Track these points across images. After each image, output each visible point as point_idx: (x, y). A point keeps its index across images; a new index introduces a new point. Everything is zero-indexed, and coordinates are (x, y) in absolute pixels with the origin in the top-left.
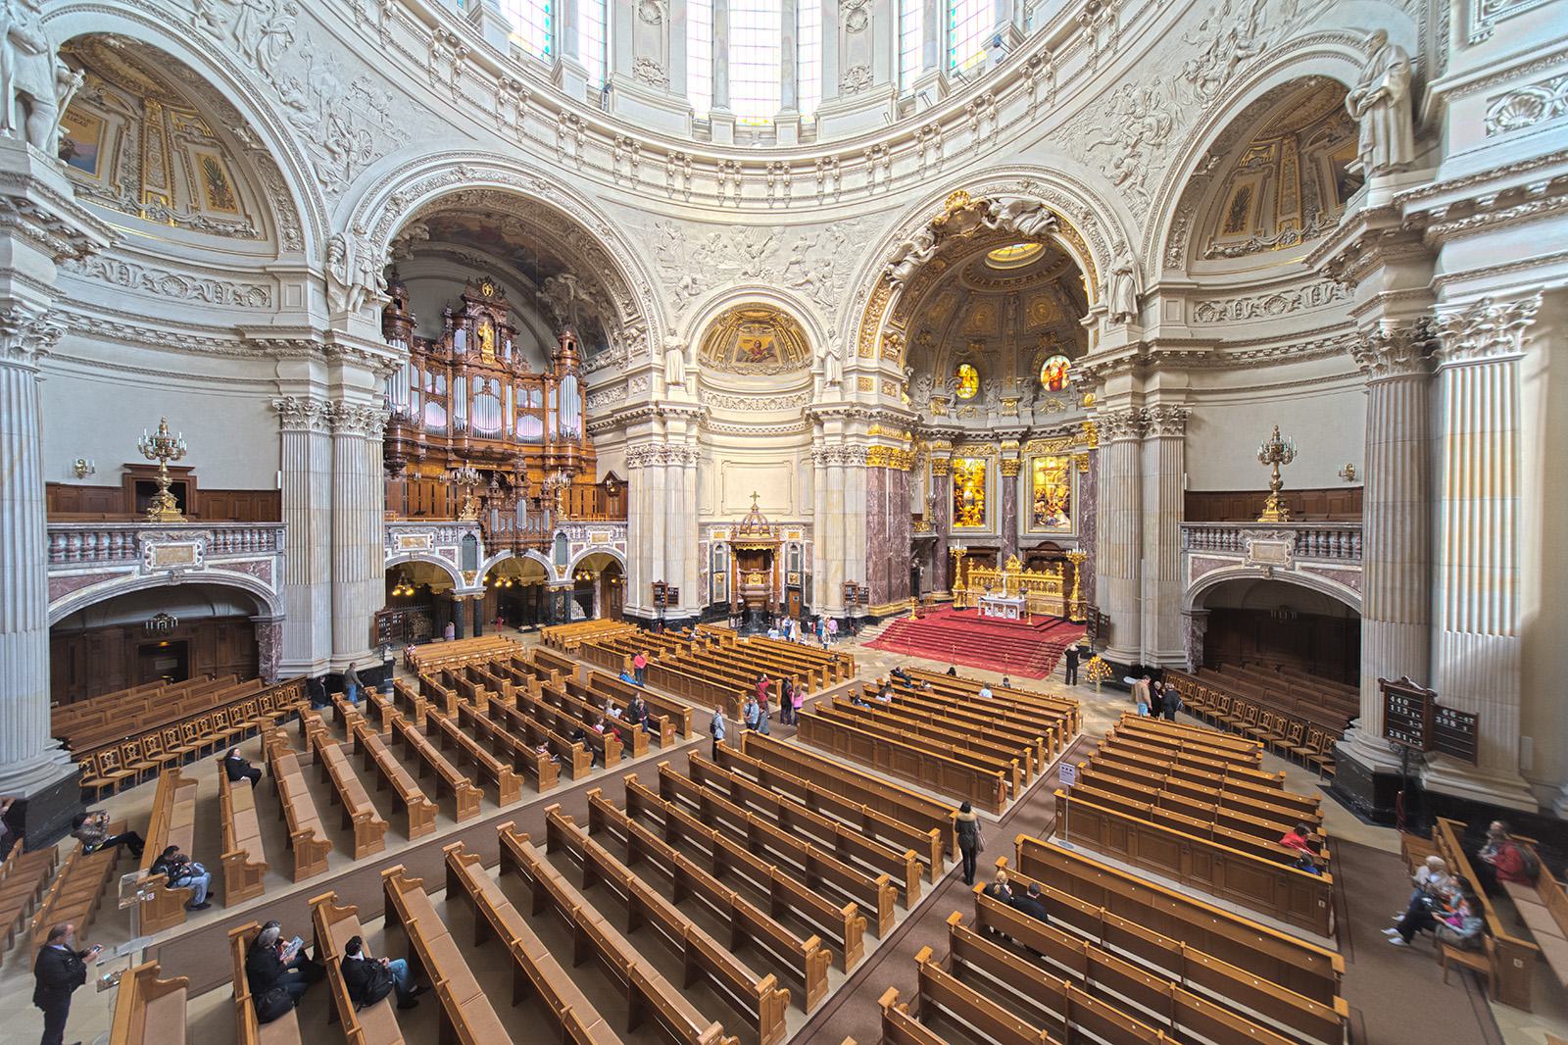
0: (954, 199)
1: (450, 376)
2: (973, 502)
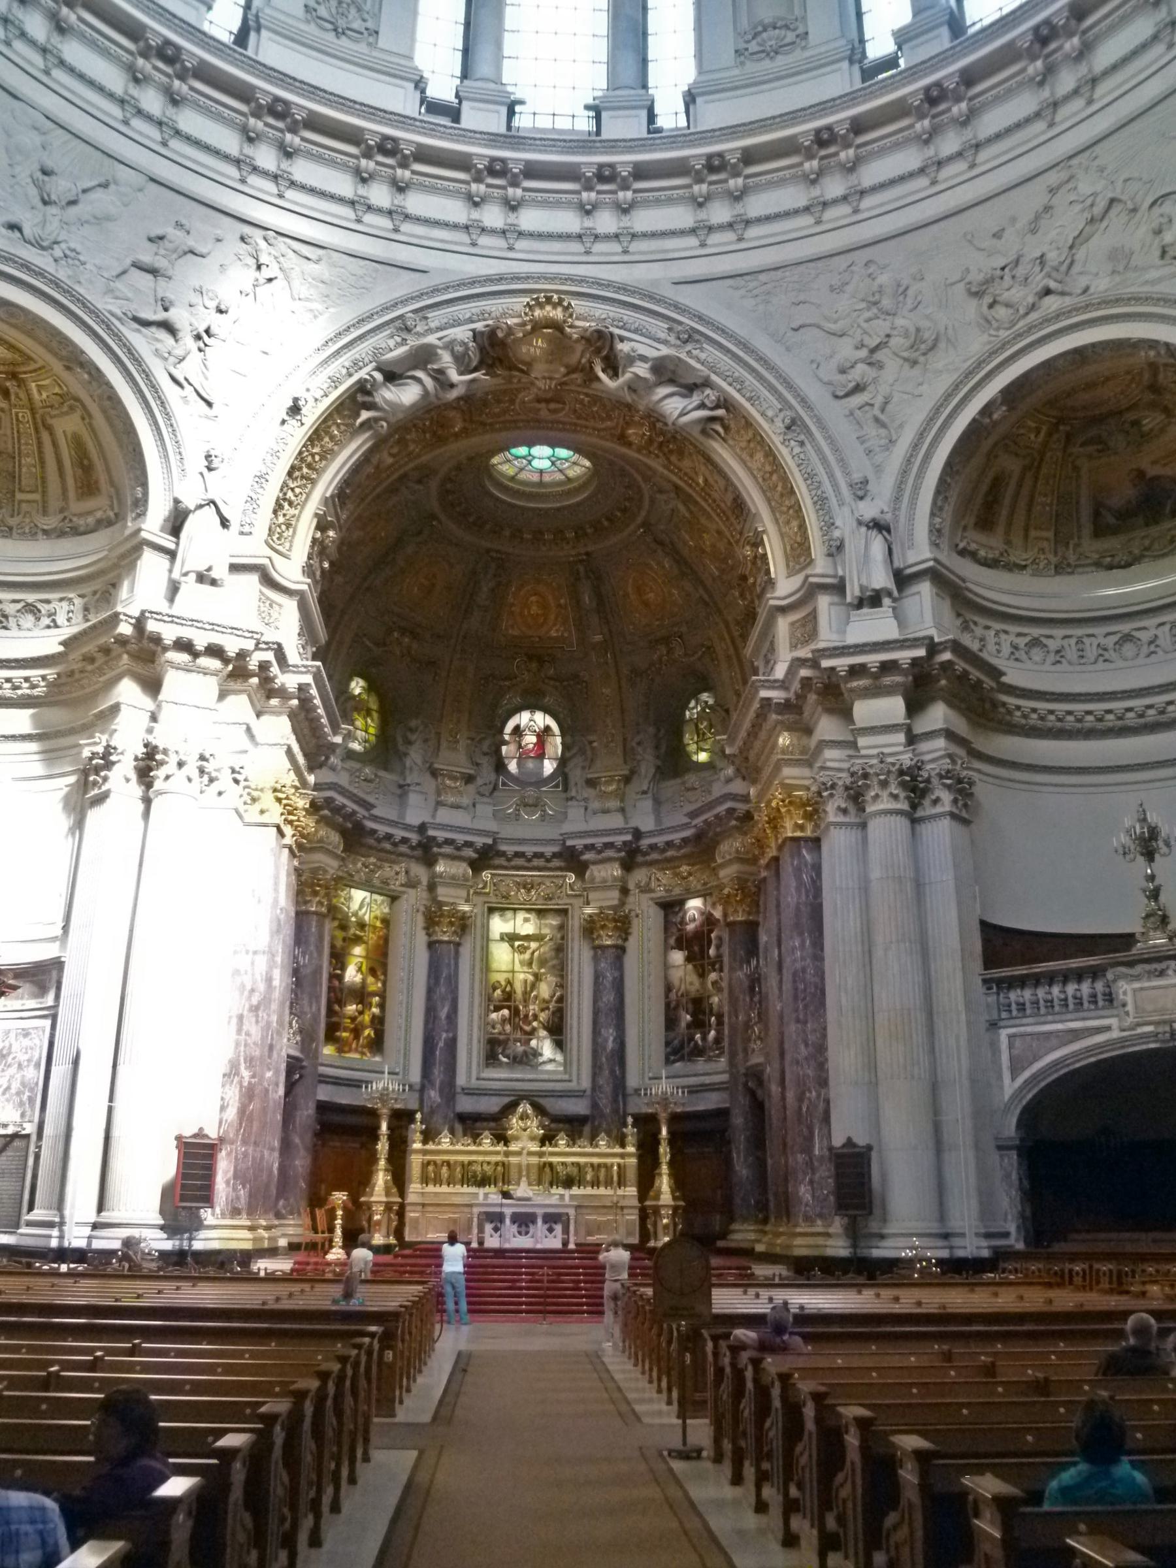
0: (541, 306)
2: (360, 995)
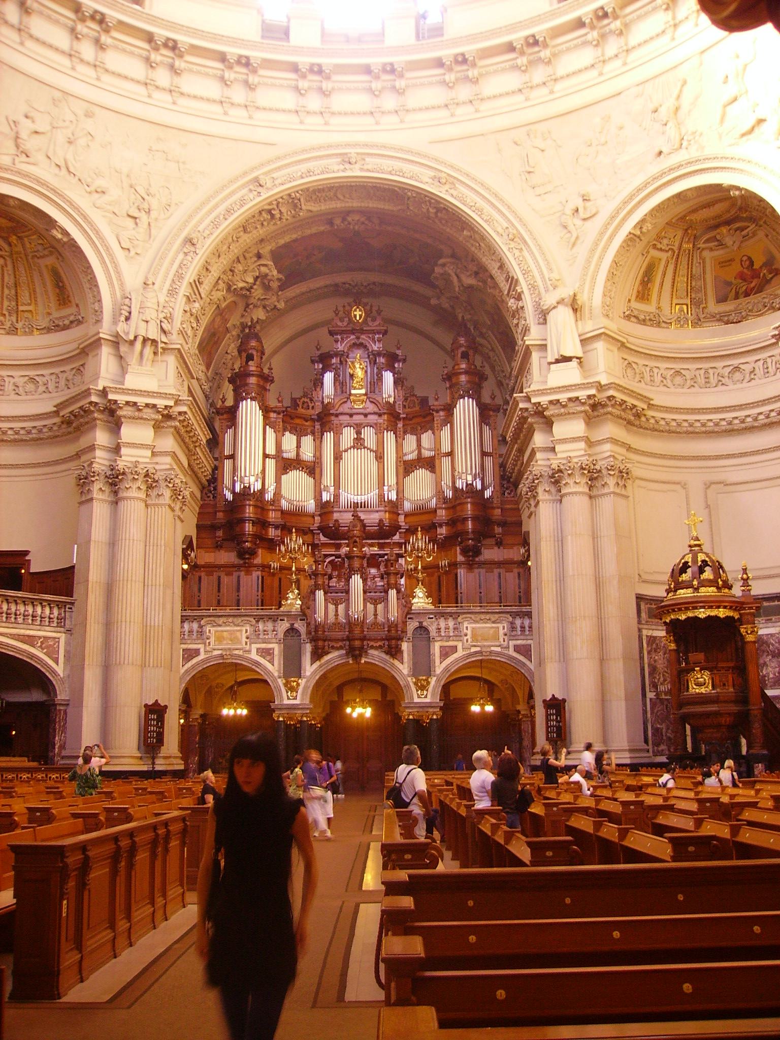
1: (318, 434)
